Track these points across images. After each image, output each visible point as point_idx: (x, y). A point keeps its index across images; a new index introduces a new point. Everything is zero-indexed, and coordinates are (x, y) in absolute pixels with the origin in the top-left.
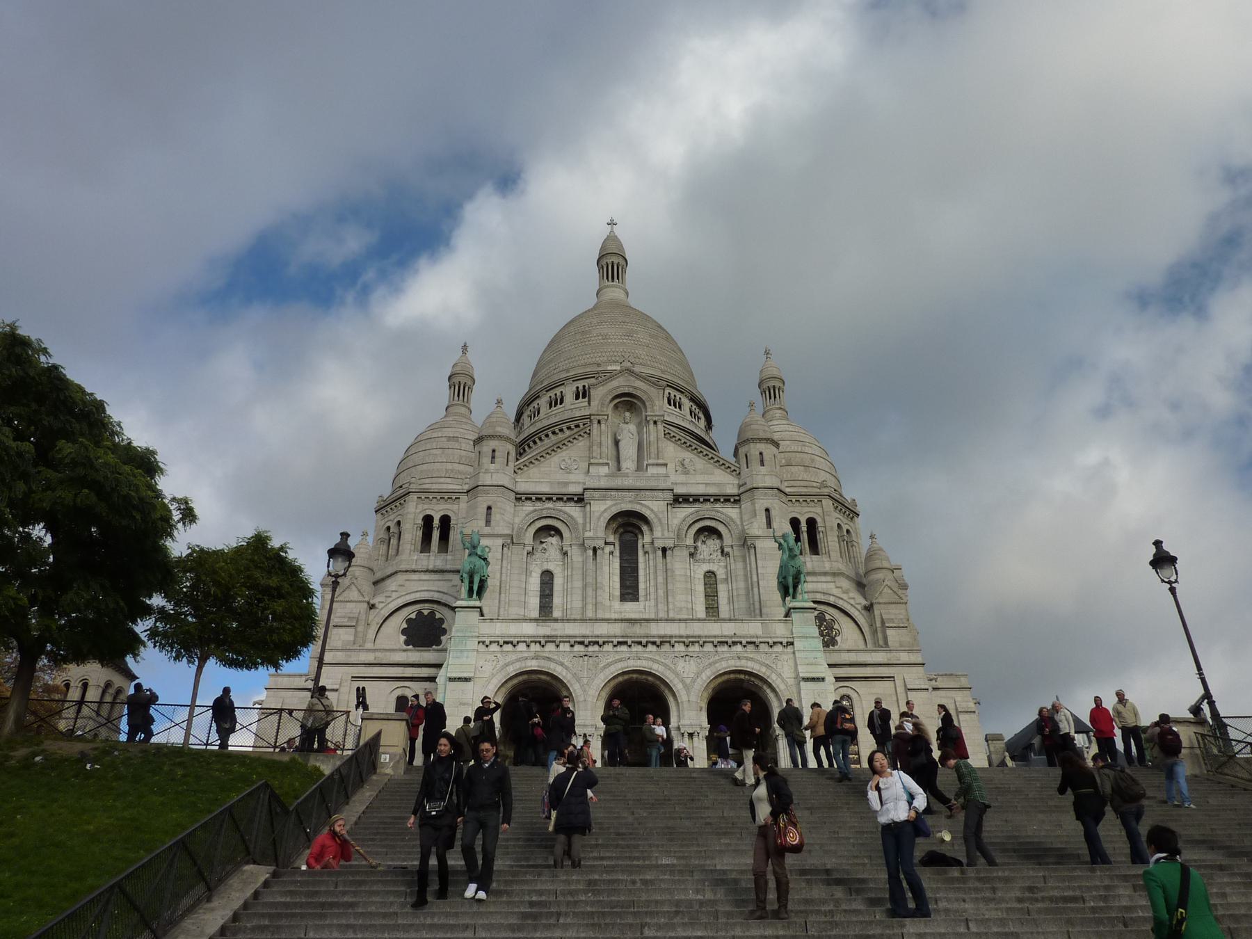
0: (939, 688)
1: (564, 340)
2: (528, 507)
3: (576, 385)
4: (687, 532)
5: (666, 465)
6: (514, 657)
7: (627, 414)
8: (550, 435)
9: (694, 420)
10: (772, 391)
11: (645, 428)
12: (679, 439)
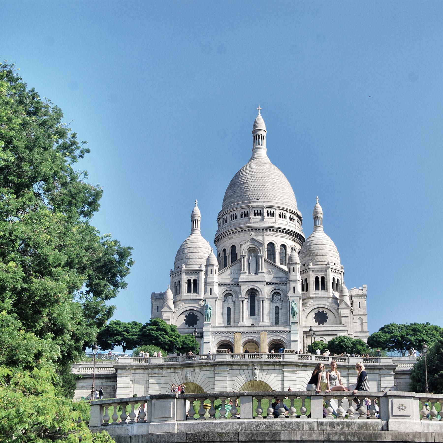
6: (220, 336)
7: (253, 254)
9: (291, 221)
10: (317, 219)
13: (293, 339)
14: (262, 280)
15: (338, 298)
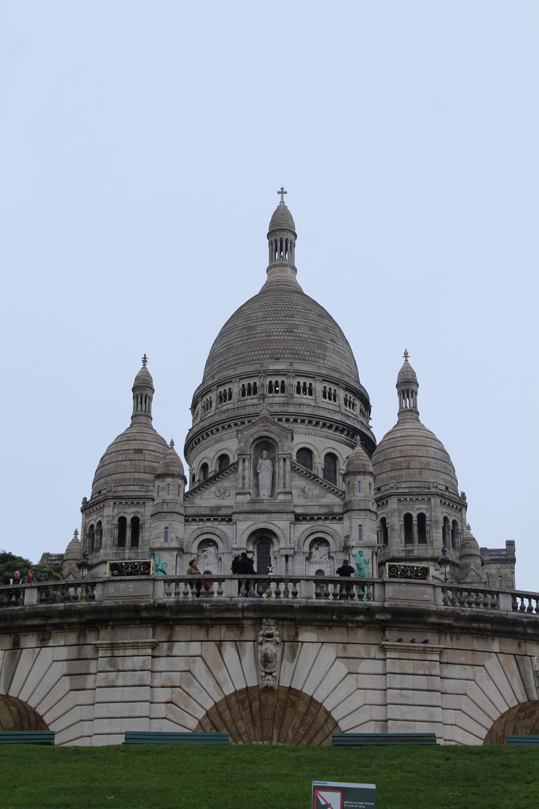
1: (232, 334)
2: (194, 526)
3: (242, 383)
4: (304, 542)
7: (265, 452)
8: (220, 430)
9: (348, 409)
10: (406, 395)
11: (277, 464)
12: (302, 471)
14: (286, 511)
15: (458, 562)
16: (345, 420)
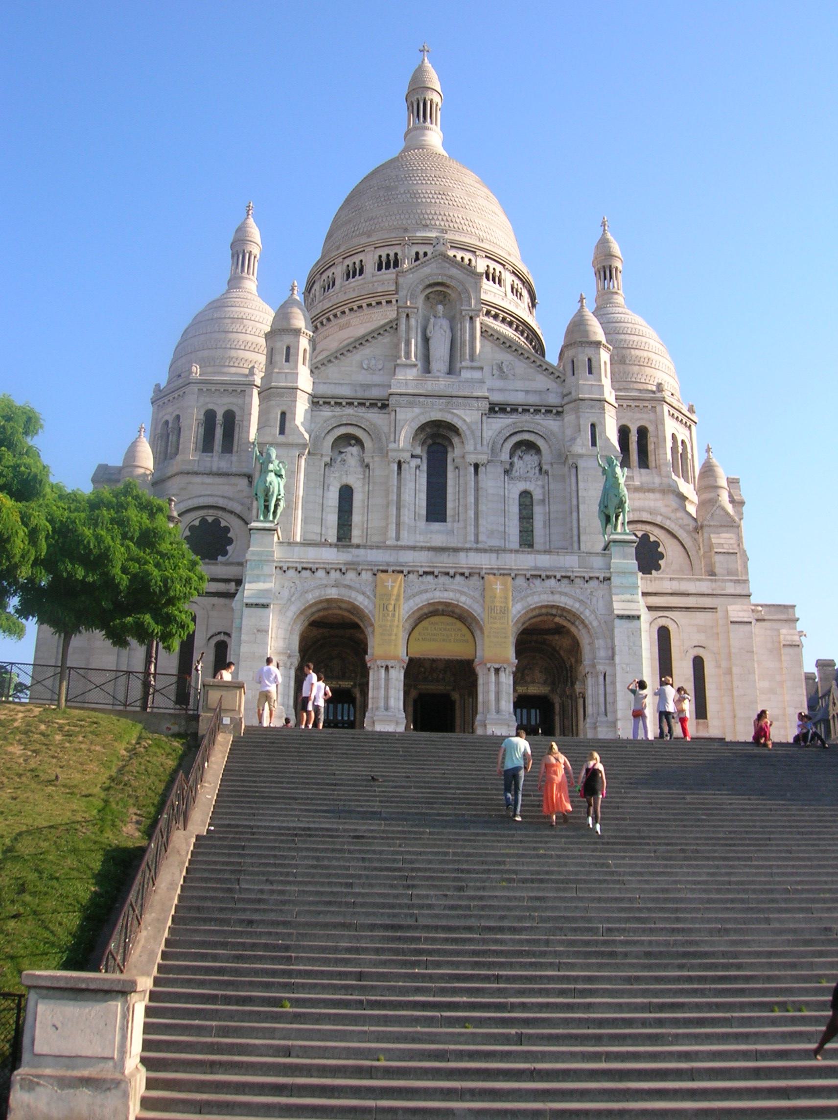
0: (764, 620)
2: (326, 412)
5: (482, 368)
7: (440, 308)
9: (515, 297)
13: (619, 608)
14: (476, 394)
16: (512, 308)
